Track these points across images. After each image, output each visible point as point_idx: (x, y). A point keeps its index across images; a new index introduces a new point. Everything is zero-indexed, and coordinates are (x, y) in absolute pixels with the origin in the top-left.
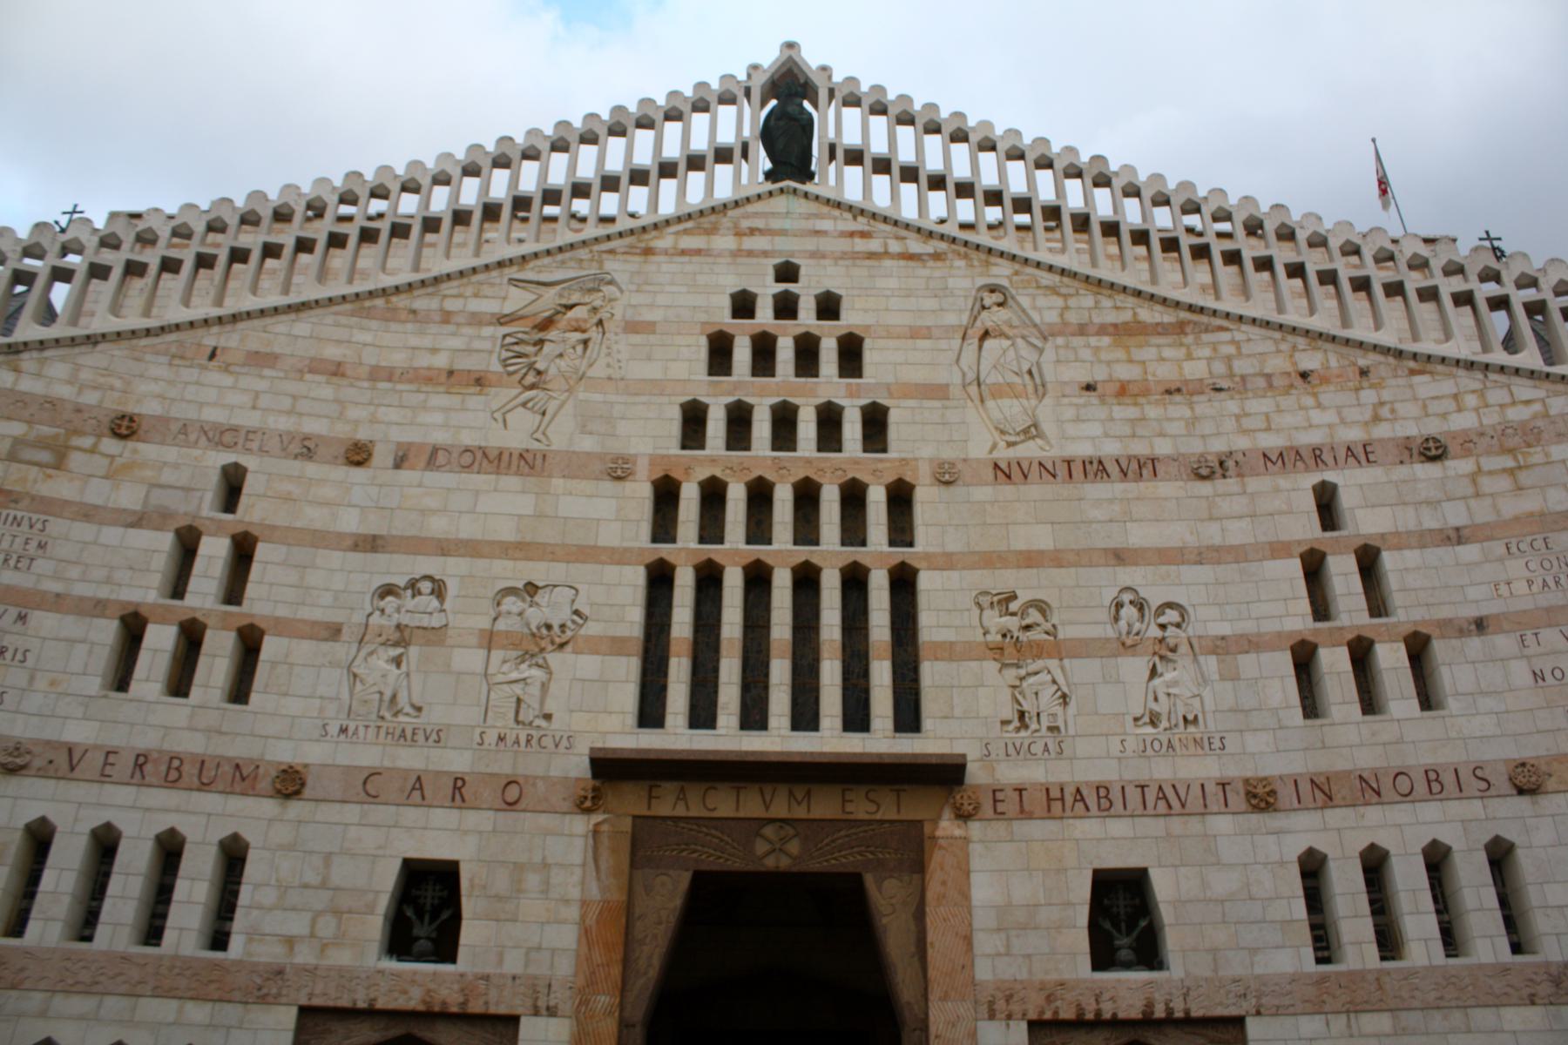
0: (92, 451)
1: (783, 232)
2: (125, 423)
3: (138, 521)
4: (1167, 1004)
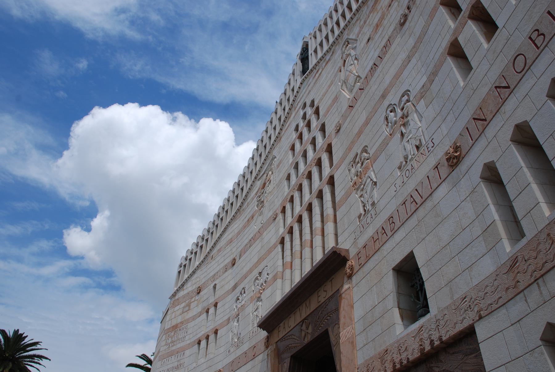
3: (200, 314)
4: (430, 338)
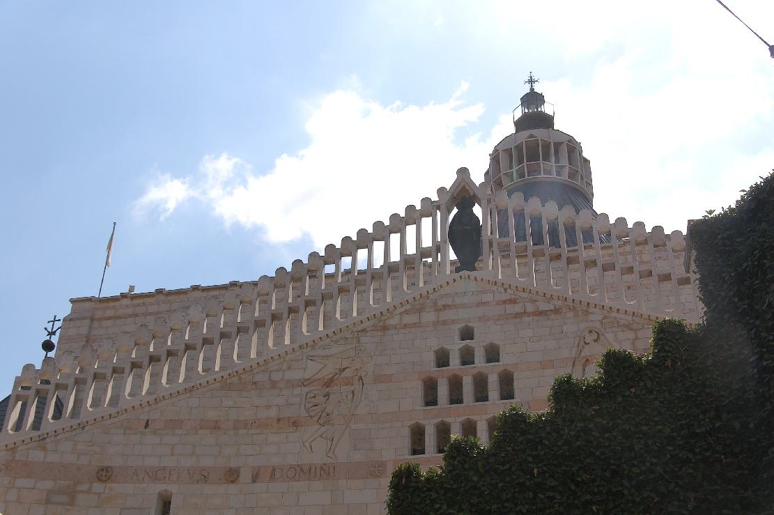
0: (89, 491)
1: (463, 306)
2: (104, 474)
